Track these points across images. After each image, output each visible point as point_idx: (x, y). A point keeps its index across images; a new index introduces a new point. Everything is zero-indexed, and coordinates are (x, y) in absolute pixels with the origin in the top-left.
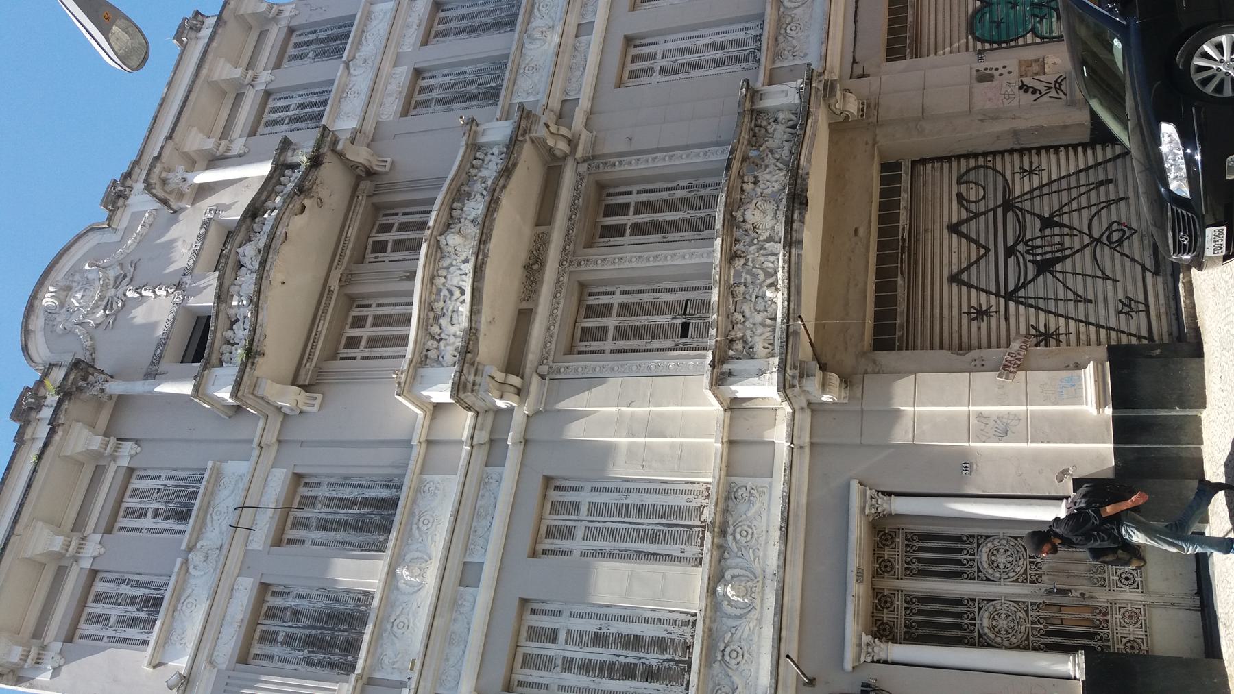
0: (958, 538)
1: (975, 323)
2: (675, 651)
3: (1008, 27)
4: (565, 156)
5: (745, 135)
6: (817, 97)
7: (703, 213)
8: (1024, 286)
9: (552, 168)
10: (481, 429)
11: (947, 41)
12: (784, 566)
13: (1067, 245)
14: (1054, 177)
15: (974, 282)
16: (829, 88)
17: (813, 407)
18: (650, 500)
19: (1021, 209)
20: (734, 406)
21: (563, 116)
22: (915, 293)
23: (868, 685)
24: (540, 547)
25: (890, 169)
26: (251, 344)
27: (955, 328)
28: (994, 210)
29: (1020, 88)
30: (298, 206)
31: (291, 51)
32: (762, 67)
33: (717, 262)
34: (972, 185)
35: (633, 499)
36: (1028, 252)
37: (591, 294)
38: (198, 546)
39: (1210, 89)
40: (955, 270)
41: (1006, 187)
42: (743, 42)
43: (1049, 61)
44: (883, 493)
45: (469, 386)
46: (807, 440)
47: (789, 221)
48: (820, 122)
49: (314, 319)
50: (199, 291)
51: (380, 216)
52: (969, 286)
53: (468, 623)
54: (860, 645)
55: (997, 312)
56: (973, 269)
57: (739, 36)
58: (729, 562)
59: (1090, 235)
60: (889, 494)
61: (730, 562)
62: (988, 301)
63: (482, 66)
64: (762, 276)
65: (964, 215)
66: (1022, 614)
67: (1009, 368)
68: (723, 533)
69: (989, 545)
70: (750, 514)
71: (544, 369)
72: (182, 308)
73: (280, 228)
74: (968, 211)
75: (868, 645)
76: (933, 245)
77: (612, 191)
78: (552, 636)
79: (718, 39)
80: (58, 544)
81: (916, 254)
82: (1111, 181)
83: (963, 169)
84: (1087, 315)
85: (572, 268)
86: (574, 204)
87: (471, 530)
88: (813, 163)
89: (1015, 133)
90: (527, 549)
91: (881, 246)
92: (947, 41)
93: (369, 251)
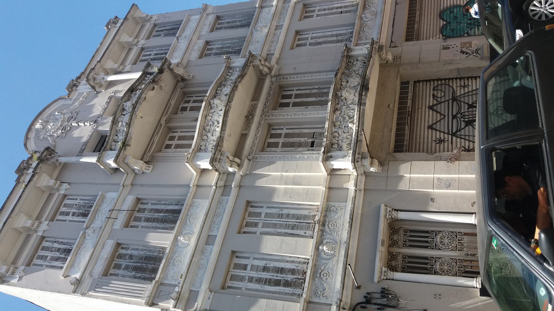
0: (427, 232)
2: (299, 275)
3: (457, 32)
4: (267, 74)
5: (344, 65)
6: (375, 51)
7: (324, 99)
8: (460, 130)
9: (261, 78)
10: (221, 180)
11: (431, 36)
12: (349, 238)
14: (474, 89)
15: (438, 128)
16: (381, 48)
17: (366, 174)
18: (292, 212)
19: (459, 101)
20: (332, 172)
21: (267, 59)
22: (413, 133)
23: (384, 289)
24: (242, 230)
25: (404, 85)
27: (429, 146)
28: (448, 101)
29: (461, 52)
30: (152, 87)
31: (154, 33)
33: (329, 111)
35: (285, 212)
36: (462, 117)
37: (273, 129)
38: (91, 227)
39: (536, 18)
40: (430, 123)
41: (454, 92)
42: (345, 34)
43: (474, 43)
44: (395, 210)
45: (218, 160)
46: (363, 187)
47: (360, 95)
48: (376, 62)
50: (103, 124)
51: (185, 96)
52: (436, 130)
53: (208, 260)
54: (381, 272)
55: (448, 141)
56: (438, 123)
58: (325, 237)
60: (397, 210)
61: (327, 237)
62: (444, 136)
63: (235, 41)
64: (347, 118)
65: (435, 102)
66: (454, 264)
67: (451, 160)
68: (324, 225)
69: (441, 234)
70: (336, 217)
71: (250, 157)
72: (96, 131)
73: (143, 95)
74: (437, 101)
75: (385, 272)
76: (421, 114)
77: (285, 89)
78: (245, 267)
79: (335, 33)
80: (29, 223)
81: (414, 117)
82: (498, 91)
83: (436, 85)
85: (266, 118)
86: (269, 93)
87: (213, 222)
89: (458, 70)
91: (399, 114)
92: (431, 36)
93: (179, 110)
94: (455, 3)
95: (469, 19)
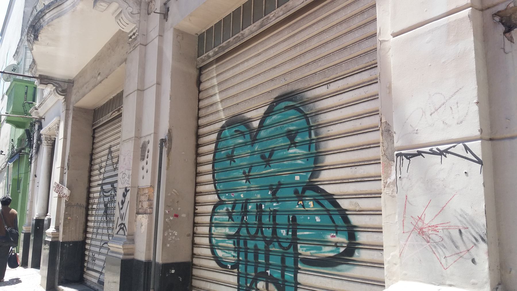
95: (259, 207)
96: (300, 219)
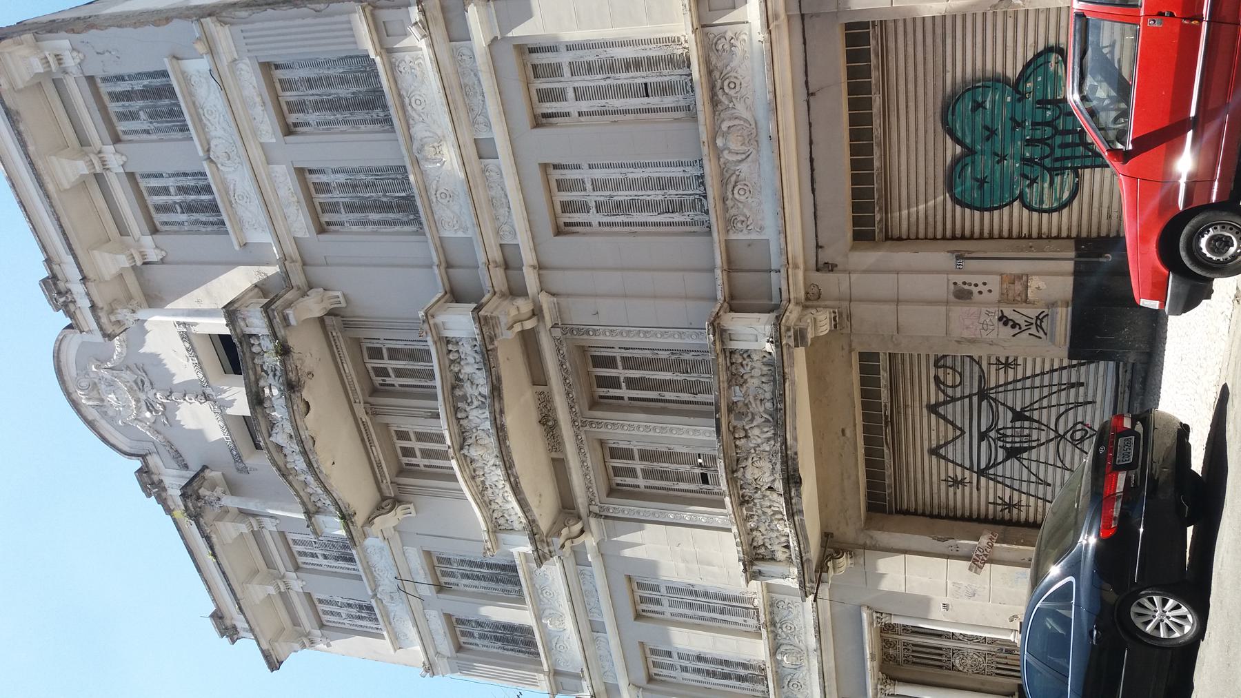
1: (951, 489)
8: (995, 465)
11: (922, 198)
13: (1035, 437)
19: (995, 400)
21: (509, 264)
22: (900, 458)
26: (341, 512)
27: (935, 490)
28: (970, 397)
29: (1000, 319)
30: (302, 407)
32: (717, 245)
34: (949, 371)
36: (999, 439)
38: (380, 589)
43: (1035, 283)
49: (363, 440)
50: (231, 403)
55: (971, 482)
57: (677, 172)
59: (1056, 431)
62: (963, 474)
65: (941, 398)
67: (977, 561)
68: (773, 624)
71: (595, 509)
73: (302, 433)
81: (899, 424)
82: (1082, 384)
84: (1045, 494)
88: (800, 438)
90: (631, 615)
91: (865, 417)
92: (922, 198)
94: (989, 67)
96: (1039, 96)
